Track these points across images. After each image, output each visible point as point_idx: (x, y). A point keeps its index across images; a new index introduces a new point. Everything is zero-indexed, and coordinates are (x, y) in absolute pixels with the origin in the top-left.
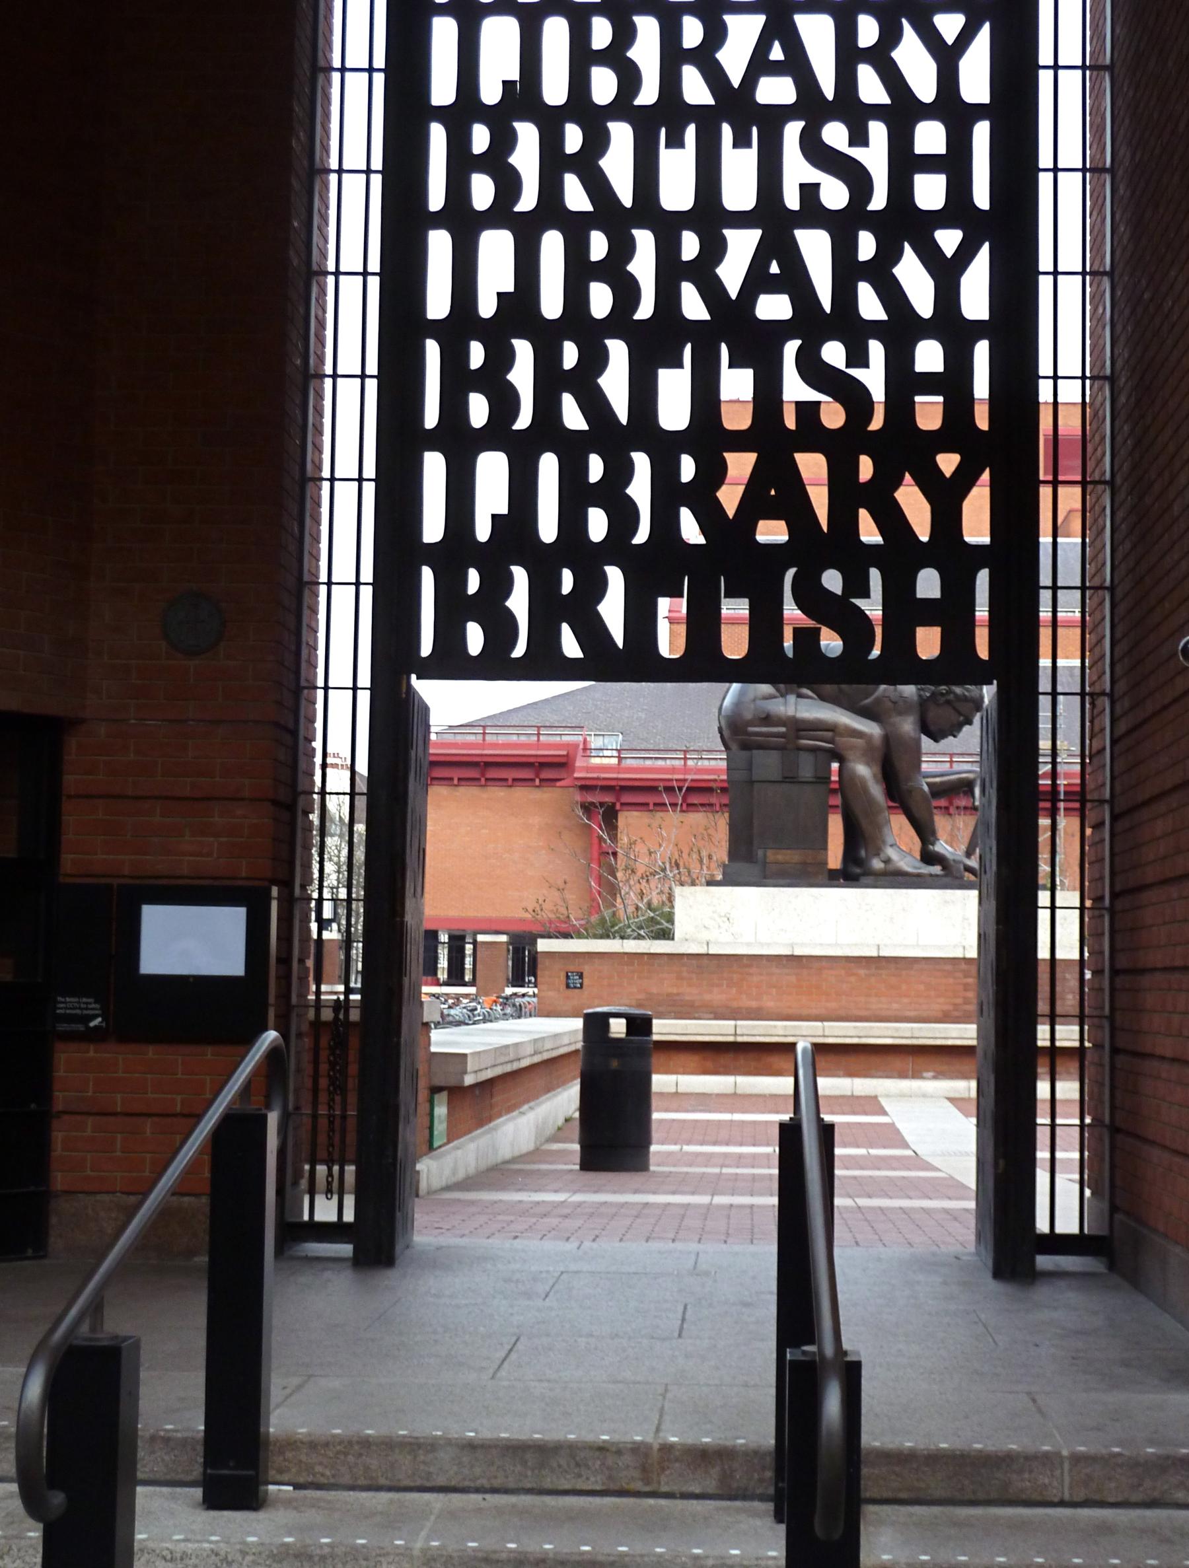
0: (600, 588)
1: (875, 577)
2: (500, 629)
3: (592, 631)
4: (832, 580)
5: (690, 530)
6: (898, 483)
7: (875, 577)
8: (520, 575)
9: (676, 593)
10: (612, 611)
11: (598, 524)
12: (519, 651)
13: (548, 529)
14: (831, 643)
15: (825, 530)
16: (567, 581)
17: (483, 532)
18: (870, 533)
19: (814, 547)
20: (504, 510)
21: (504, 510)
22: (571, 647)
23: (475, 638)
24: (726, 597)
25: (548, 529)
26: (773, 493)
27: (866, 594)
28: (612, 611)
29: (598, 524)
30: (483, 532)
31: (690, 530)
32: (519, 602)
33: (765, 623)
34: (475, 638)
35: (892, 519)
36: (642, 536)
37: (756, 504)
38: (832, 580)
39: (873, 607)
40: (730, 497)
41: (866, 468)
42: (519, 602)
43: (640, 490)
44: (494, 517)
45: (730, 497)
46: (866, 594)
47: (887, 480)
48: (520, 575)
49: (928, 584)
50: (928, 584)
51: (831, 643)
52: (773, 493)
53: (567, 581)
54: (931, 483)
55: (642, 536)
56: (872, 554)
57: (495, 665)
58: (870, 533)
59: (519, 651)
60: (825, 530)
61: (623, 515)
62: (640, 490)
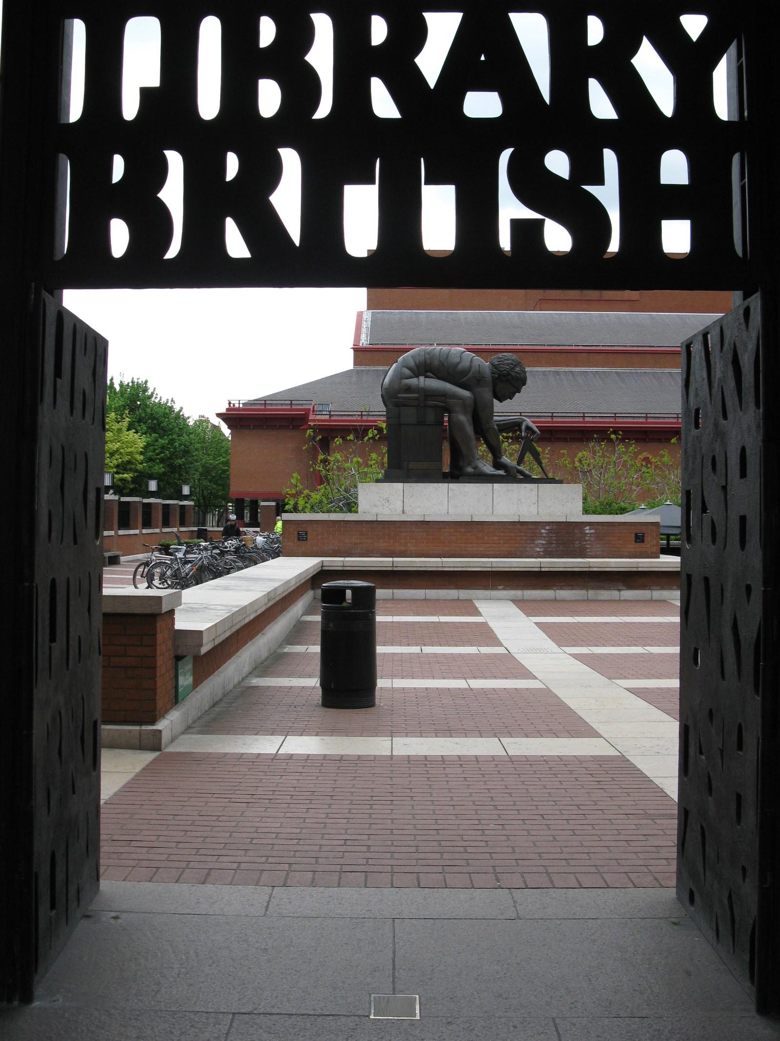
0: (273, 173)
1: (610, 158)
2: (150, 224)
3: (262, 226)
4: (558, 162)
5: (383, 103)
6: (634, 49)
7: (610, 158)
8: (175, 160)
9: (369, 180)
10: (287, 201)
11: (269, 97)
12: (174, 250)
13: (209, 103)
14: (557, 238)
15: (546, 97)
16: (232, 165)
17: (130, 109)
18: (601, 105)
19: (533, 122)
20: (154, 80)
21: (154, 80)
22: (236, 245)
23: (119, 237)
24: (426, 183)
25: (209, 103)
26: (483, 58)
27: (599, 180)
28: (287, 201)
29: (269, 97)
30: (130, 109)
31: (383, 103)
32: (173, 194)
33: (476, 213)
34: (119, 237)
35: (629, 90)
36: (324, 110)
37: (462, 71)
38: (558, 162)
39: (608, 194)
40: (431, 62)
41: (595, 31)
42: (173, 194)
43: (321, 56)
44: (145, 93)
45: (431, 62)
46: (599, 180)
47: (620, 47)
48: (175, 160)
49: (674, 167)
50: (674, 167)
51: (557, 238)
52: (483, 58)
53: (232, 165)
54: (674, 49)
55: (324, 110)
56: (605, 133)
57: (146, 269)
58: (601, 105)
59: (174, 250)
60: (546, 97)
61: (300, 86)
62: (321, 56)
